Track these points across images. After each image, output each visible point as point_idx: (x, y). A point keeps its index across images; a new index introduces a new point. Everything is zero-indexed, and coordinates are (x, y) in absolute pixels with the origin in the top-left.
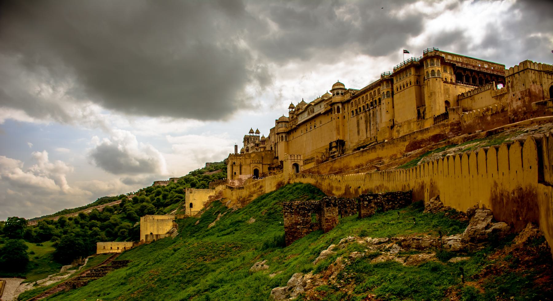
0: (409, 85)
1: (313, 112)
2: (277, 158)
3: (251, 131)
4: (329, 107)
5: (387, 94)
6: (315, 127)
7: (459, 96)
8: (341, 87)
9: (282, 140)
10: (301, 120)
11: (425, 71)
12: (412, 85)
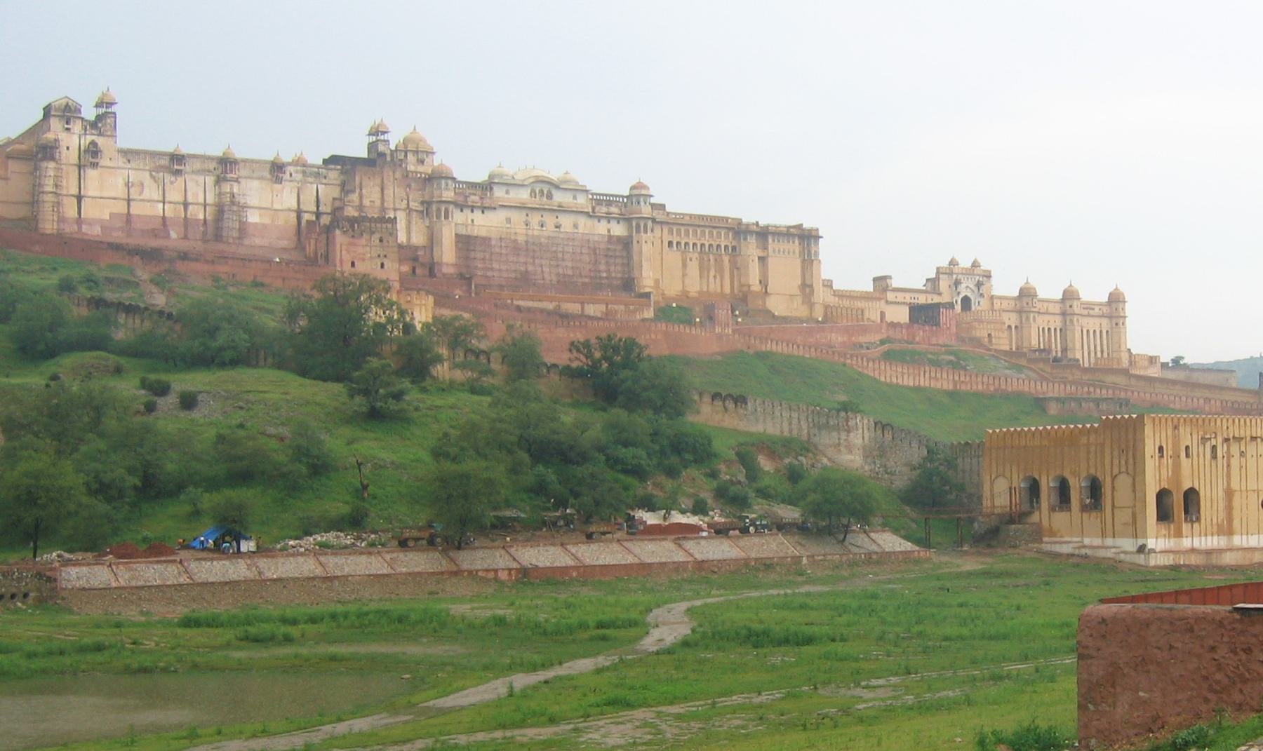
1: (550, 196)
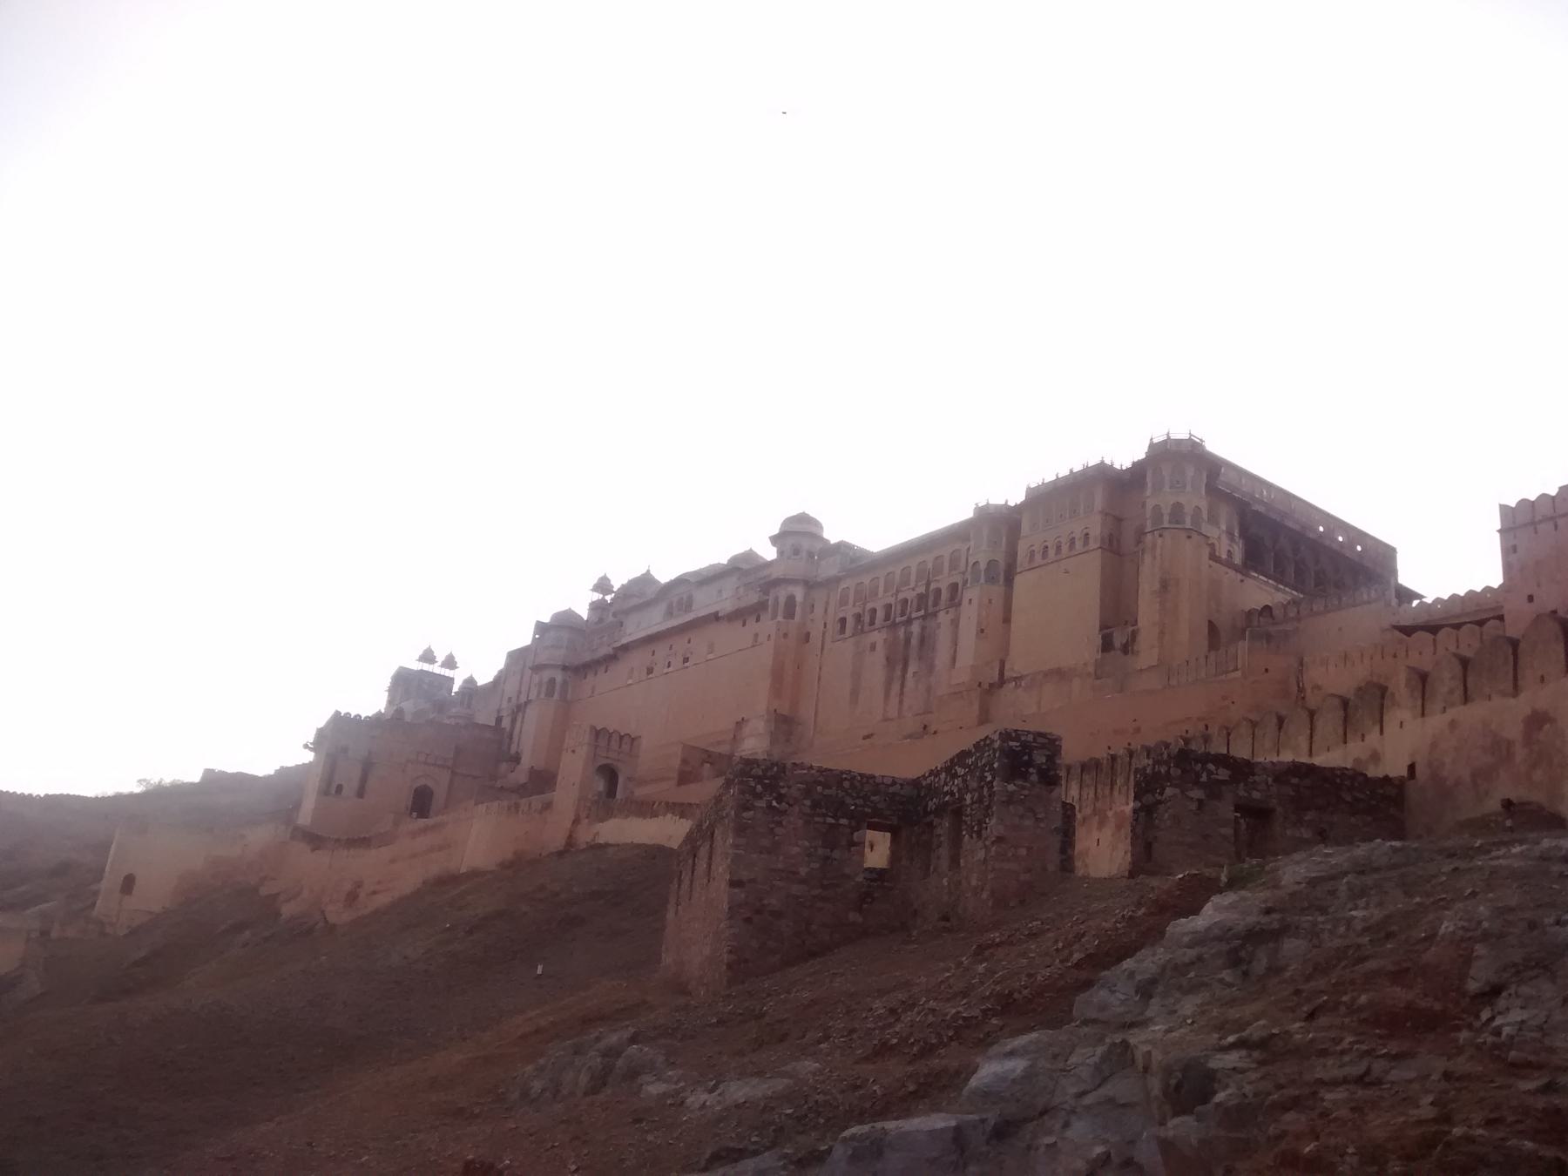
0: (1079, 545)
1: (688, 605)
2: (516, 759)
3: (428, 657)
4: (753, 598)
5: (987, 570)
6: (686, 660)
7: (1250, 613)
8: (813, 529)
9: (550, 693)
10: (635, 630)
11: (1150, 504)
12: (1093, 545)
